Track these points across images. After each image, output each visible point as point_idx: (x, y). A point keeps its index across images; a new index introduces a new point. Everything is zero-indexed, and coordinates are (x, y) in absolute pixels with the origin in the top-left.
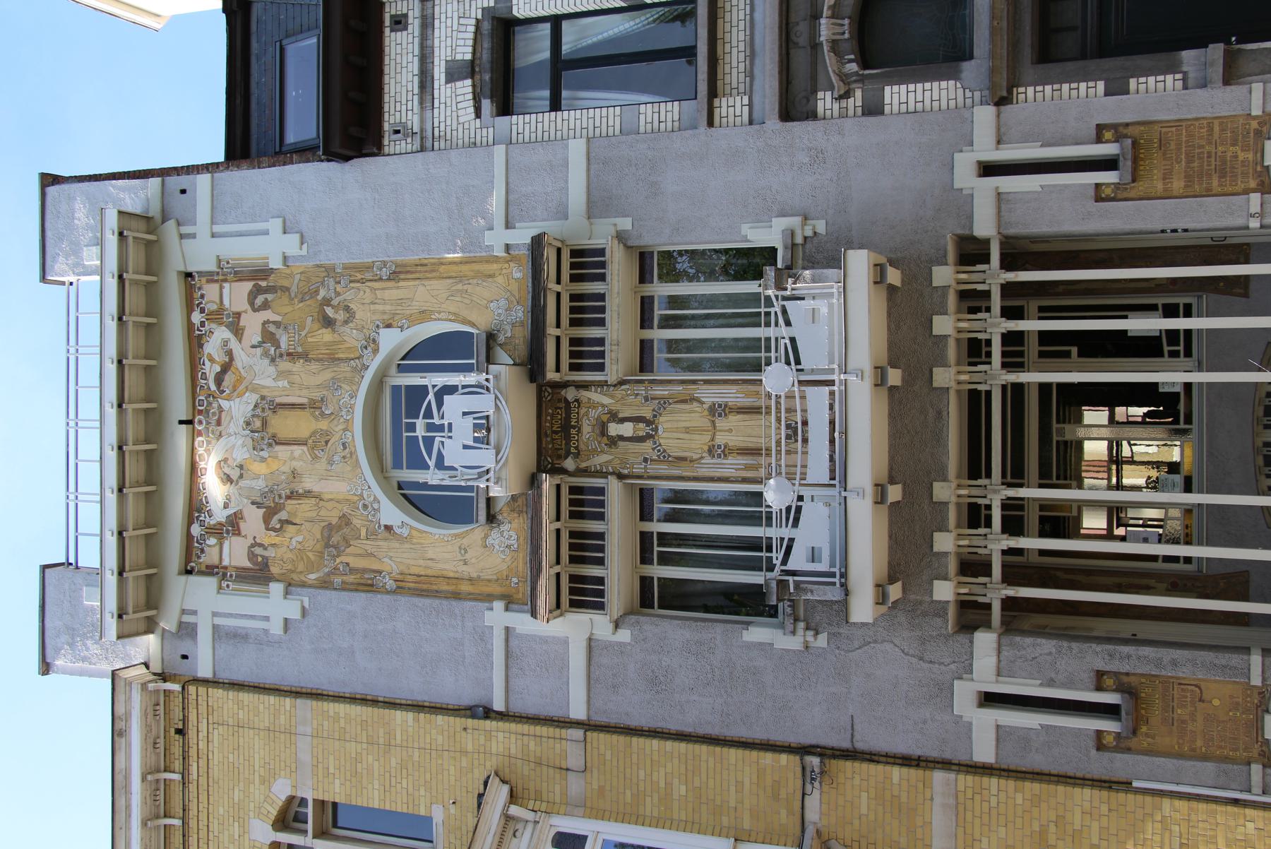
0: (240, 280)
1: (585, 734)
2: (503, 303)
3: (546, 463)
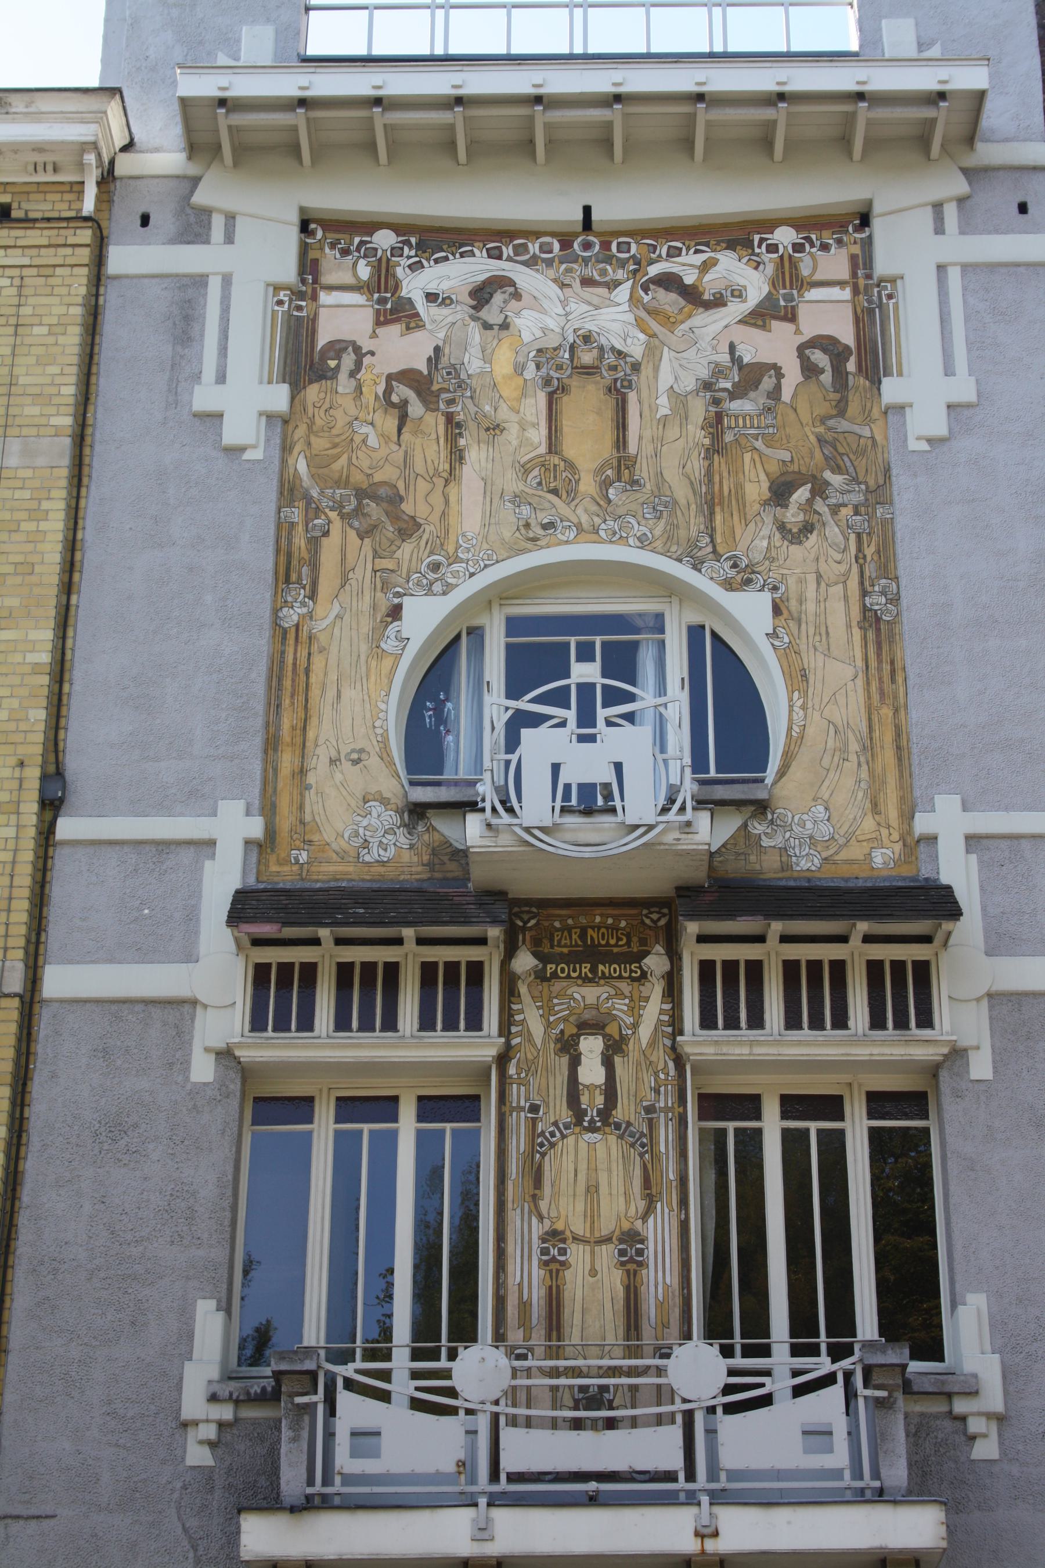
0: (857, 320)
1: (16, 995)
2: (825, 830)
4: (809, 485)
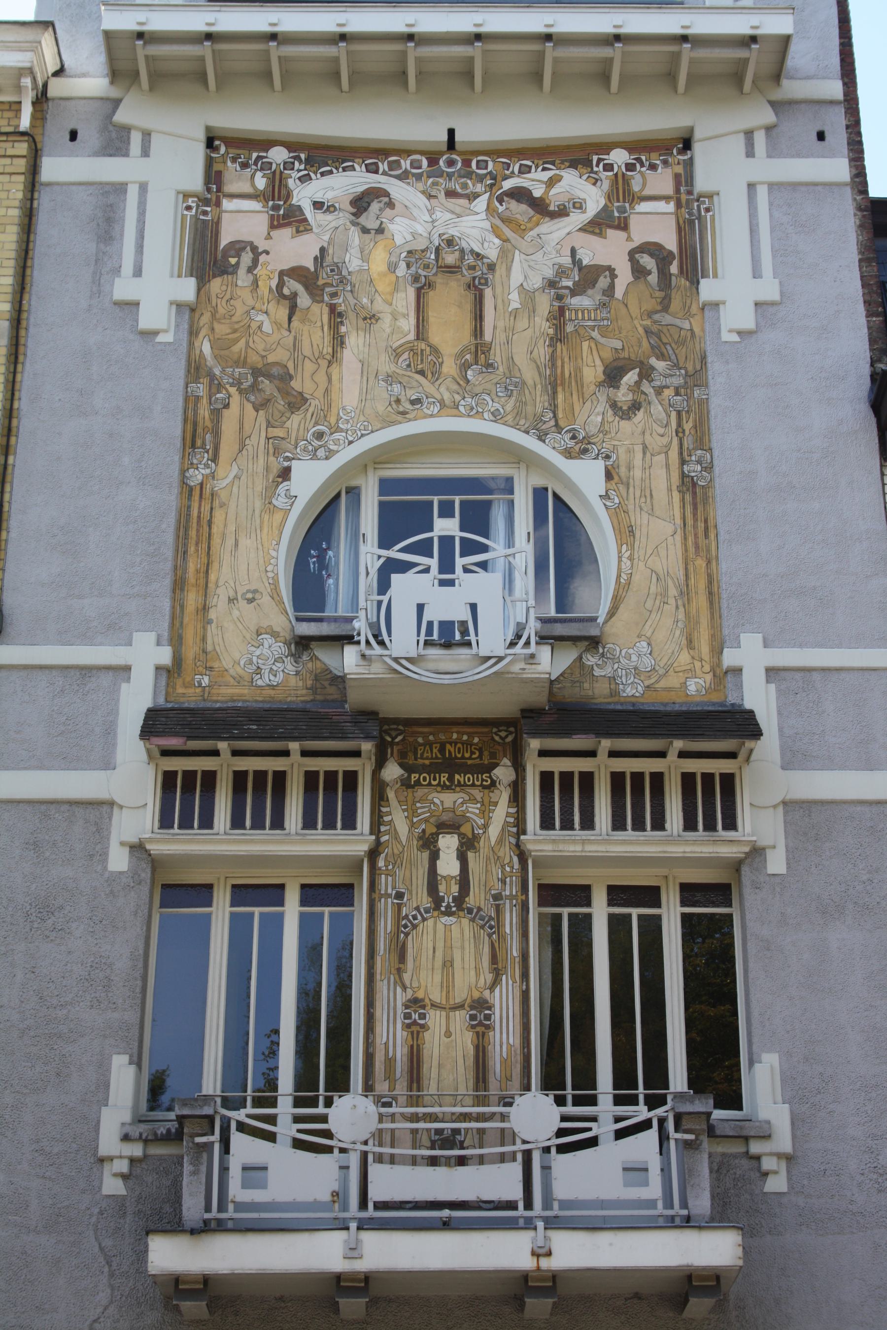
0: (679, 230)
2: (647, 663)
4: (638, 370)
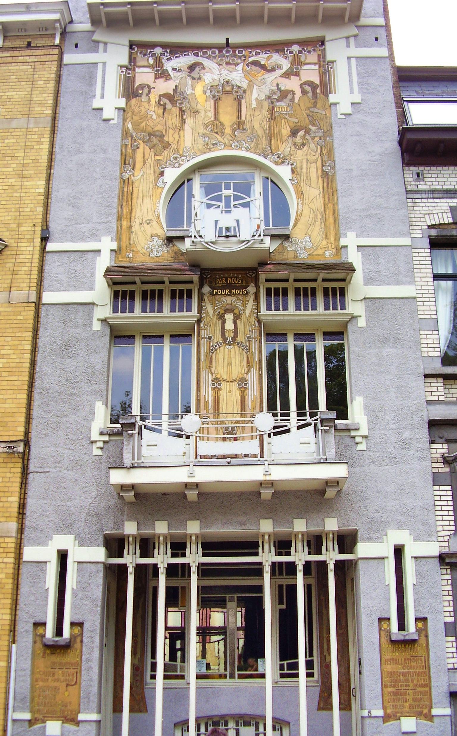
0: (320, 76)
2: (309, 244)
3: (207, 274)
